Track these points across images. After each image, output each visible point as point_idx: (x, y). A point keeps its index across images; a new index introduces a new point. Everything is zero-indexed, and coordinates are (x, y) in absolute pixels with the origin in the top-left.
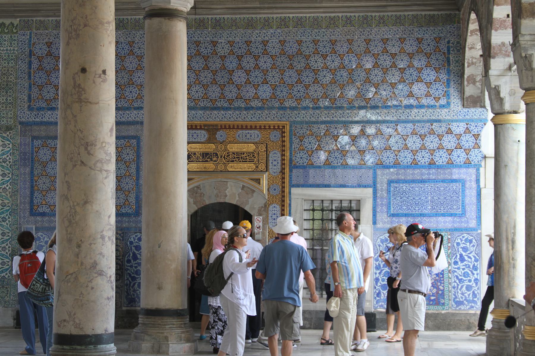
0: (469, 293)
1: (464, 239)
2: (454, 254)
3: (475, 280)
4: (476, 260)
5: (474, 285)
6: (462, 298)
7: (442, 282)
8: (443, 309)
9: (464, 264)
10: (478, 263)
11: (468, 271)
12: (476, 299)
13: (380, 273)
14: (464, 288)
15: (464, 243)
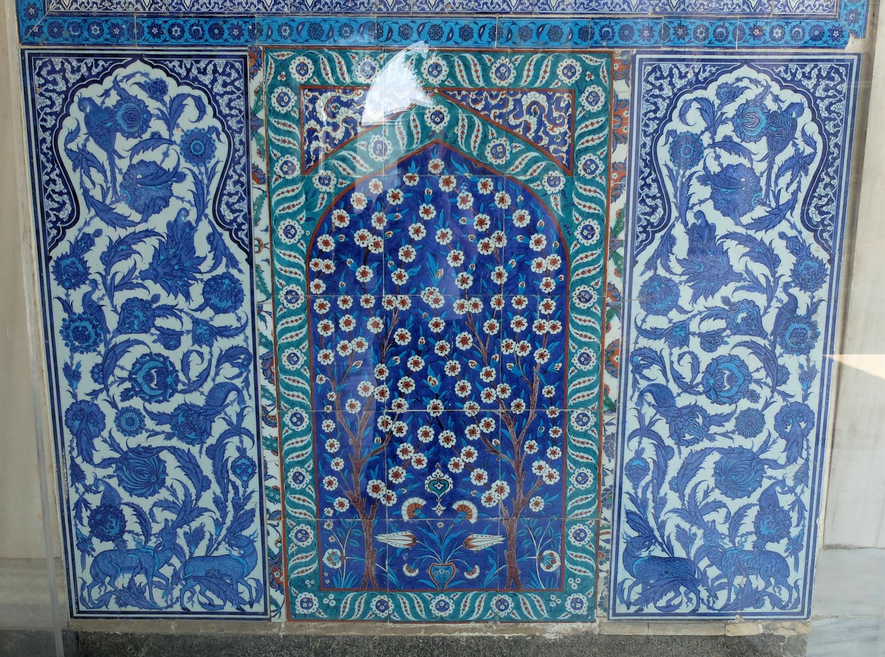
0: (734, 505)
1: (730, 110)
2: (649, 231)
3: (782, 420)
4: (808, 276)
5: (777, 452)
6: (686, 539)
7: (555, 432)
8: (555, 614)
9: (716, 301)
10: (822, 293)
11: (743, 353)
12: (779, 547)
13: (101, 373)
14: (706, 474)
15: (728, 144)
